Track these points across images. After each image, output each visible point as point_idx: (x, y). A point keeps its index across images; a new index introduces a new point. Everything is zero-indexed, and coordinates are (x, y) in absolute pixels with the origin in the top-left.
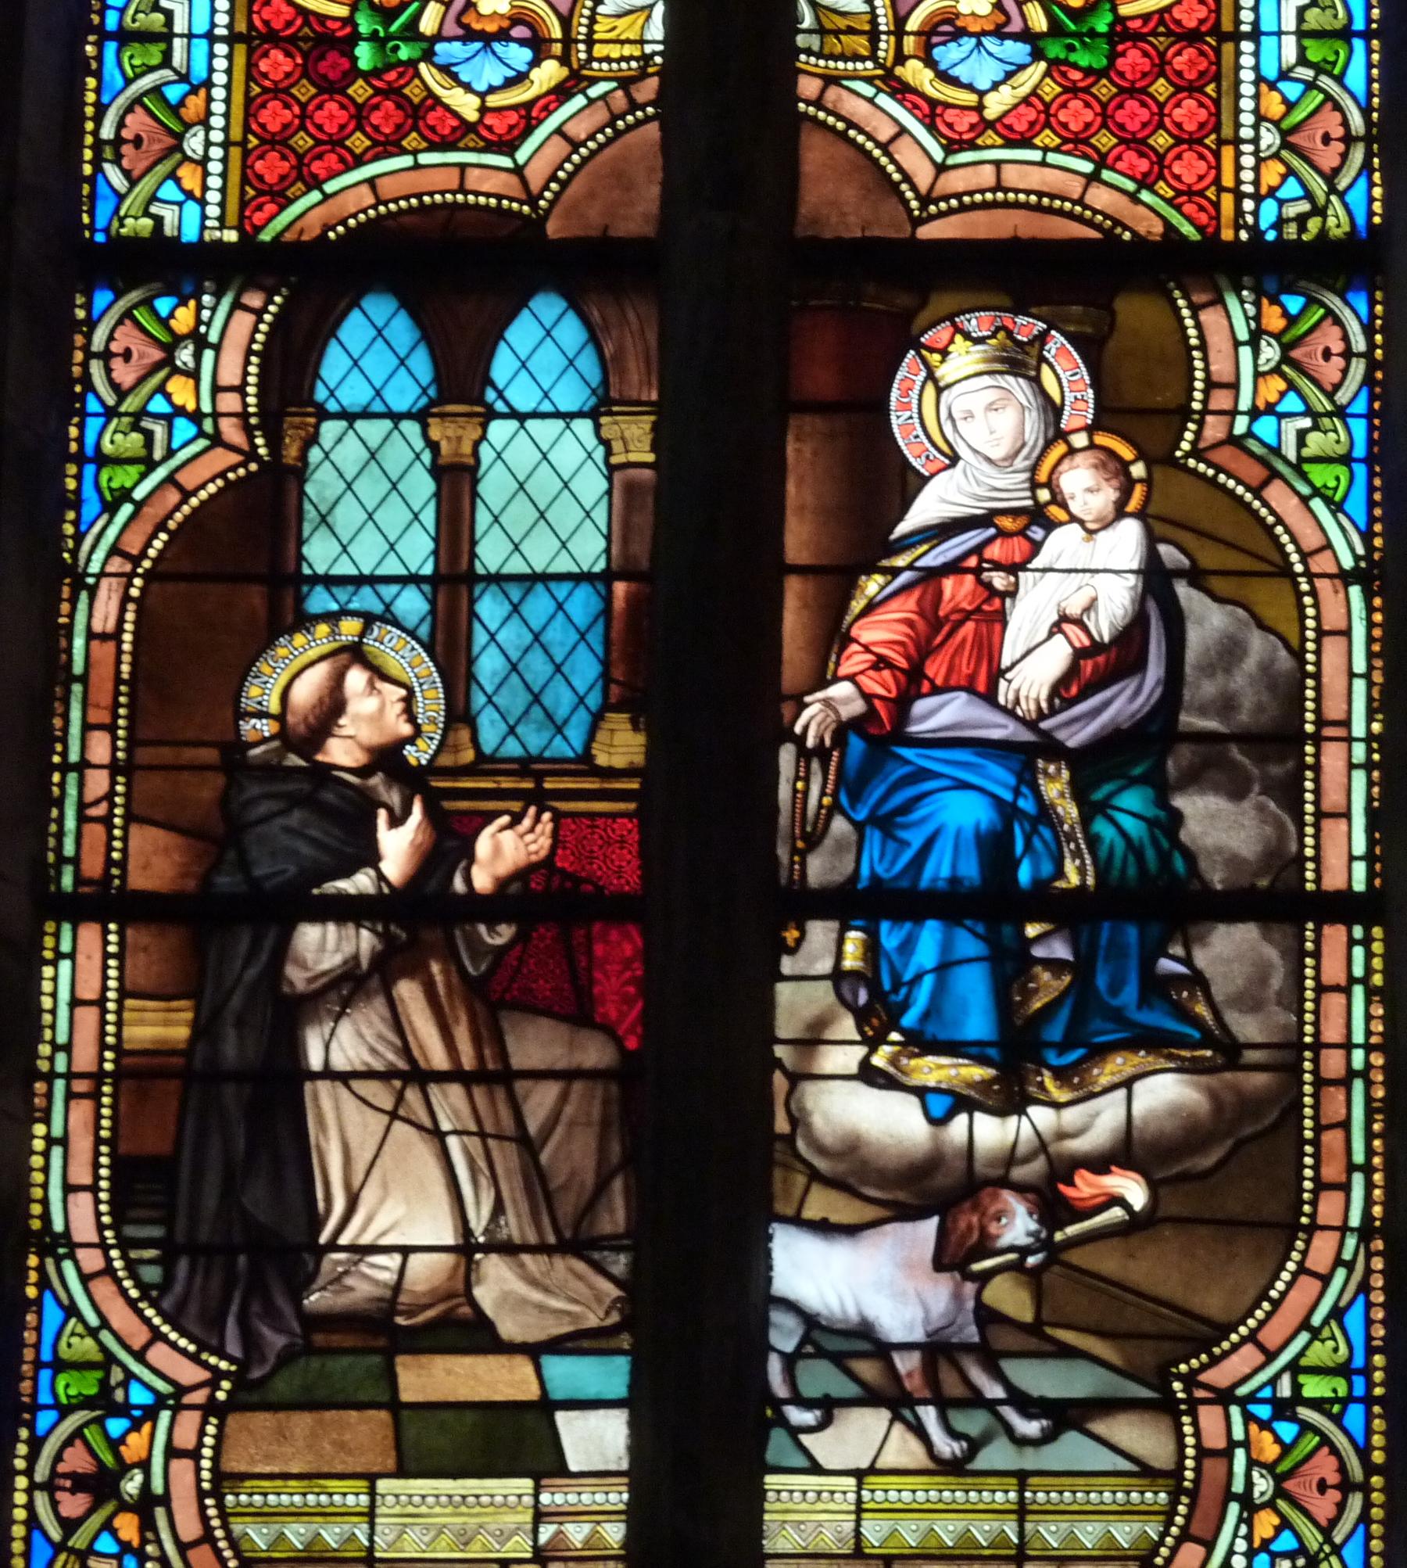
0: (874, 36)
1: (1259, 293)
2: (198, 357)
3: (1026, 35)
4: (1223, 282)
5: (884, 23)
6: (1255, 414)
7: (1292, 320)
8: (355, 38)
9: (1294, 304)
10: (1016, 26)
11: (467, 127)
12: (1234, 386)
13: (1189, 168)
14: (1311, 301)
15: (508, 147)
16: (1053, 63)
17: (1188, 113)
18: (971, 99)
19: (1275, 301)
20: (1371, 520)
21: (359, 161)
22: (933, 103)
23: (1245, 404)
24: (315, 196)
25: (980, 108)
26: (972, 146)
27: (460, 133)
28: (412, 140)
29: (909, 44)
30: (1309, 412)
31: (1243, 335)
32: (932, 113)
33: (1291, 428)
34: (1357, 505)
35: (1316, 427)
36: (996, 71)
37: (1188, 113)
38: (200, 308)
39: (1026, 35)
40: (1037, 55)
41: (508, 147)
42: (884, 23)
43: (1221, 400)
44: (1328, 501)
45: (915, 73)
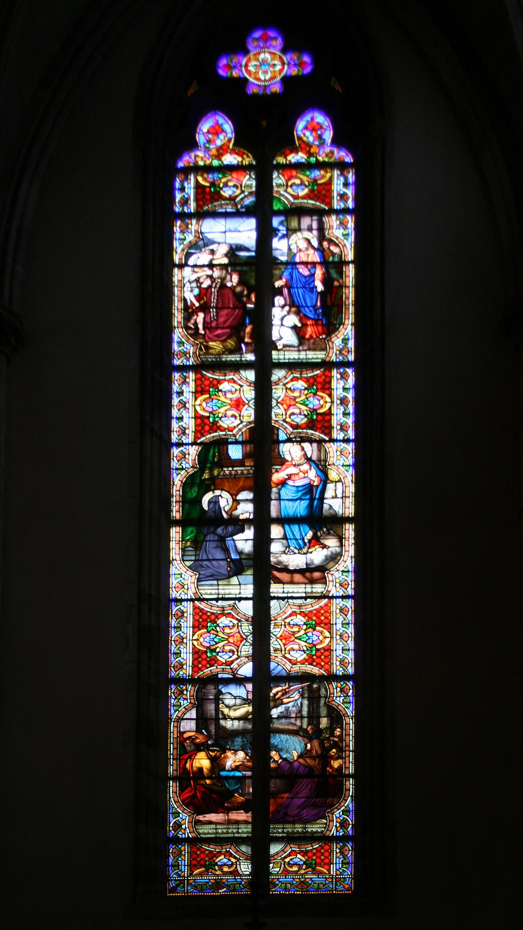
0: (281, 651)
1: (337, 682)
2: (187, 692)
3: (304, 651)
4: (331, 680)
5: (283, 649)
6: (336, 697)
7: (342, 685)
8: (207, 652)
9: (342, 683)
10: (302, 649)
11: (223, 663)
12: (334, 694)
13: (327, 667)
14: (344, 683)
15: (229, 665)
16: (307, 654)
17: (327, 660)
18: (296, 659)
19: (339, 683)
20: (353, 710)
21: (208, 668)
22: (290, 659)
23: (335, 695)
24: (202, 672)
25: (297, 660)
26: (296, 664)
27: (222, 664)
28: (216, 665)
29: (286, 652)
30: (344, 696)
31: (335, 687)
32: (290, 660)
33: (342, 699)
34: (351, 708)
35: (345, 698)
36: (299, 655)
37: (327, 660)
38: (187, 686)
39: (304, 651)
40: (305, 653)
41: (229, 665)
42: (283, 649)
43: (332, 695)
44: (347, 708)
45: (287, 655)
